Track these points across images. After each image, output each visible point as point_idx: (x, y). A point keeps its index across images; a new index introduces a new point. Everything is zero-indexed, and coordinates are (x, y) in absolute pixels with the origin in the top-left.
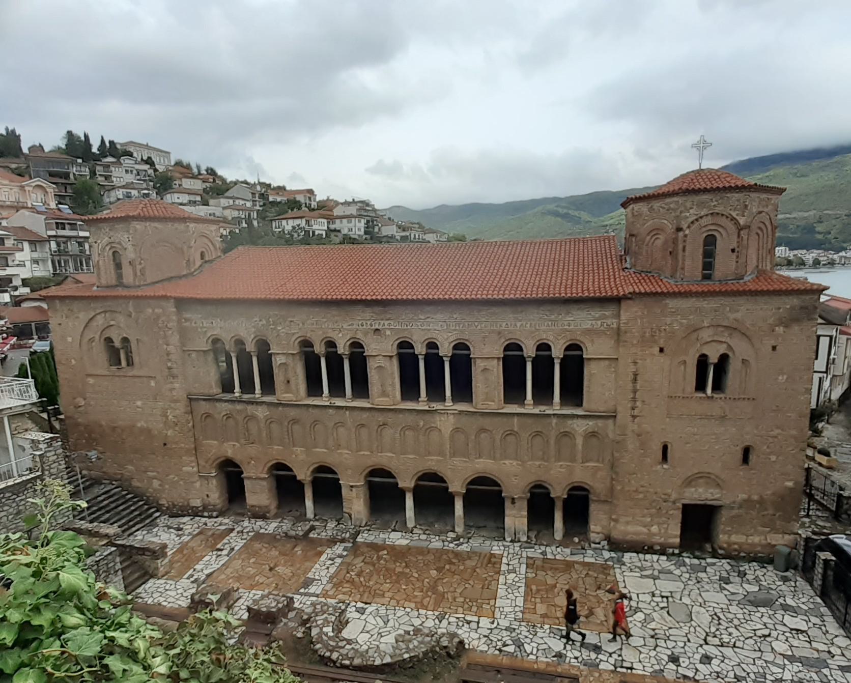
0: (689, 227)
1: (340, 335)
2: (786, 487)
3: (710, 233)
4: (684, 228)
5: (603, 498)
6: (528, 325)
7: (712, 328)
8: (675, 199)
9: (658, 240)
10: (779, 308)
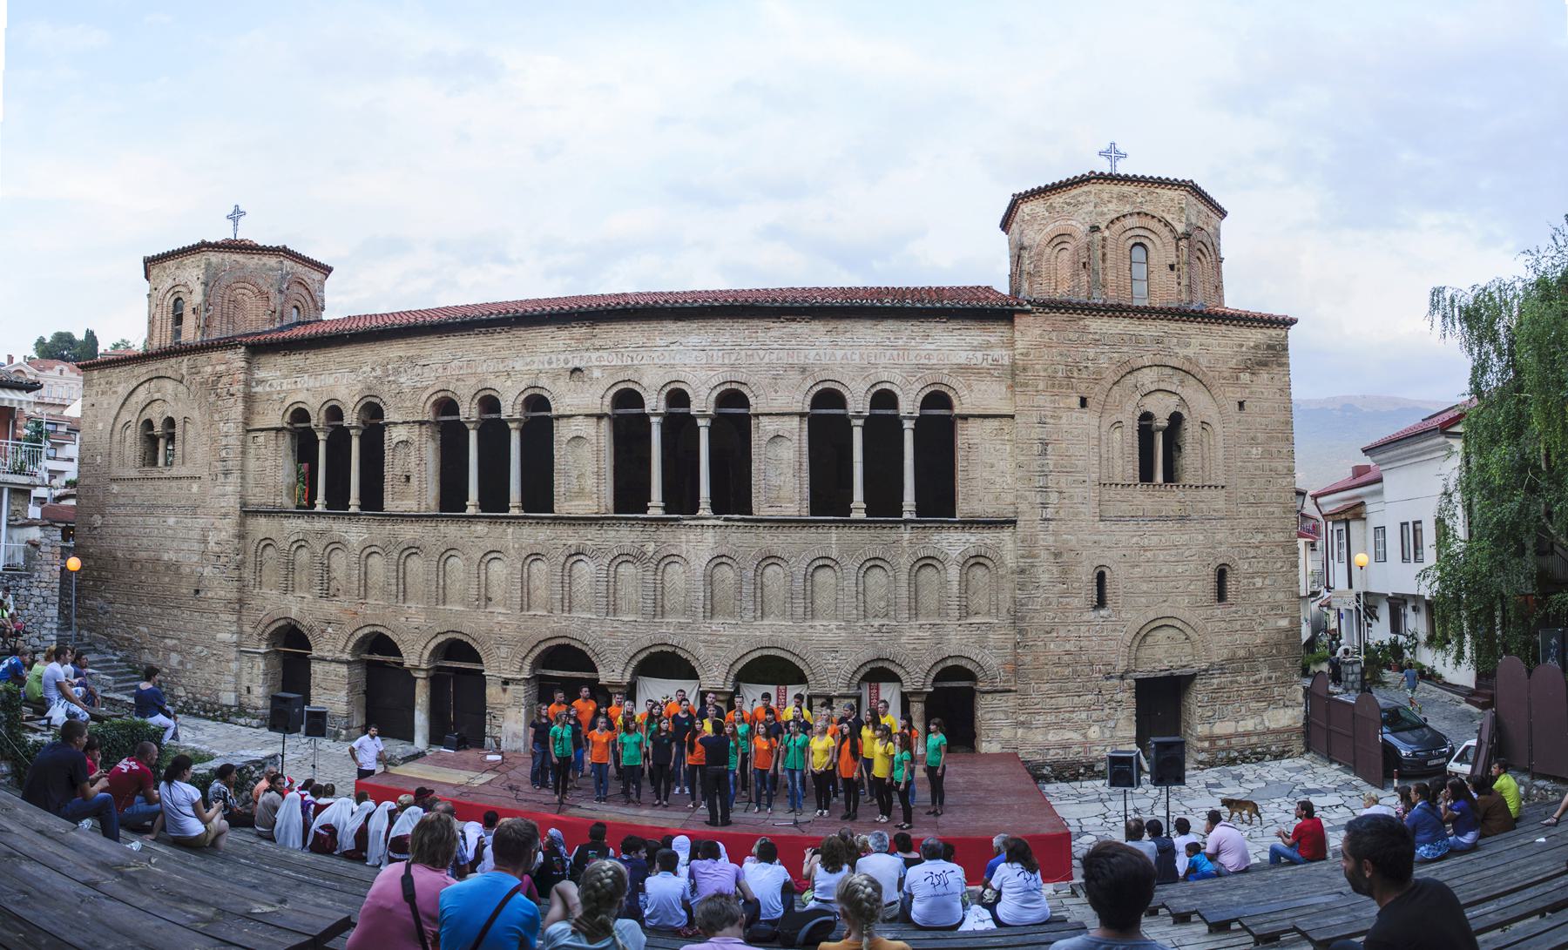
1: (509, 383)
5: (1000, 686)
6: (856, 357)
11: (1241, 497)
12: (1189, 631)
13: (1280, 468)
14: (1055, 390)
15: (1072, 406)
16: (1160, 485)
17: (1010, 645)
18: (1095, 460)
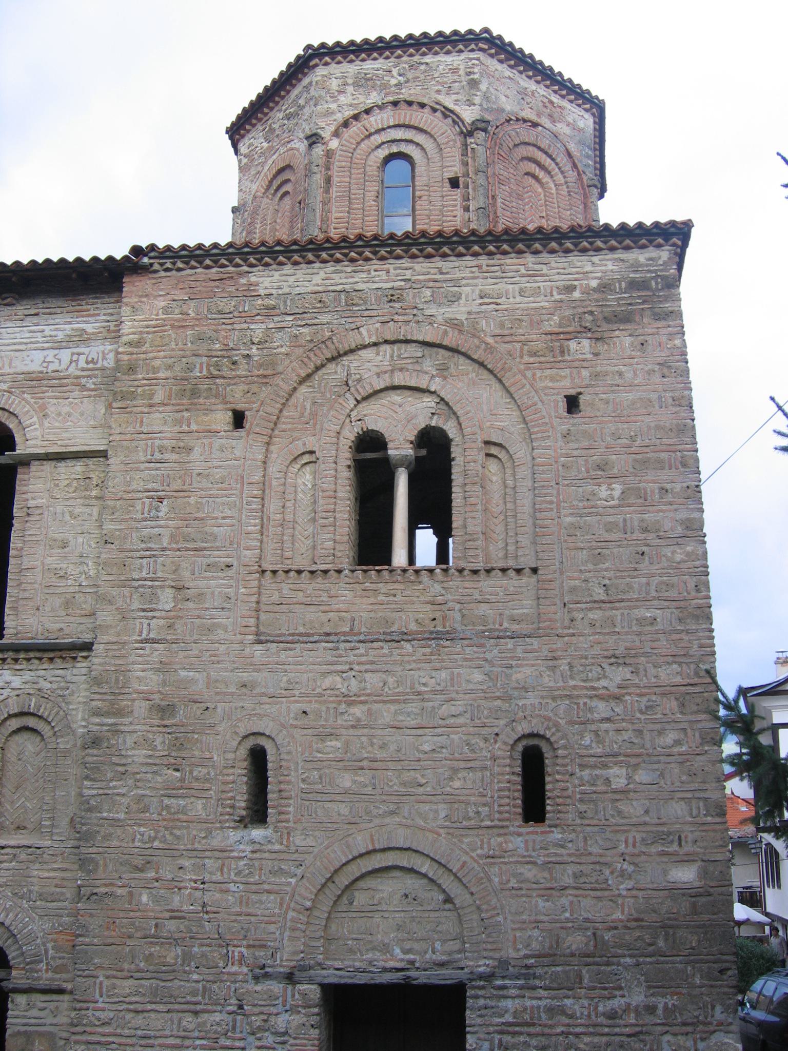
0: (336, 134)
2: (675, 891)
3: (395, 149)
4: (326, 134)
5: (45, 977)
7: (387, 347)
10: (570, 289)
11: (573, 590)
12: (447, 882)
13: (668, 525)
14: (185, 401)
15: (214, 427)
17: (69, 894)
18: (253, 527)
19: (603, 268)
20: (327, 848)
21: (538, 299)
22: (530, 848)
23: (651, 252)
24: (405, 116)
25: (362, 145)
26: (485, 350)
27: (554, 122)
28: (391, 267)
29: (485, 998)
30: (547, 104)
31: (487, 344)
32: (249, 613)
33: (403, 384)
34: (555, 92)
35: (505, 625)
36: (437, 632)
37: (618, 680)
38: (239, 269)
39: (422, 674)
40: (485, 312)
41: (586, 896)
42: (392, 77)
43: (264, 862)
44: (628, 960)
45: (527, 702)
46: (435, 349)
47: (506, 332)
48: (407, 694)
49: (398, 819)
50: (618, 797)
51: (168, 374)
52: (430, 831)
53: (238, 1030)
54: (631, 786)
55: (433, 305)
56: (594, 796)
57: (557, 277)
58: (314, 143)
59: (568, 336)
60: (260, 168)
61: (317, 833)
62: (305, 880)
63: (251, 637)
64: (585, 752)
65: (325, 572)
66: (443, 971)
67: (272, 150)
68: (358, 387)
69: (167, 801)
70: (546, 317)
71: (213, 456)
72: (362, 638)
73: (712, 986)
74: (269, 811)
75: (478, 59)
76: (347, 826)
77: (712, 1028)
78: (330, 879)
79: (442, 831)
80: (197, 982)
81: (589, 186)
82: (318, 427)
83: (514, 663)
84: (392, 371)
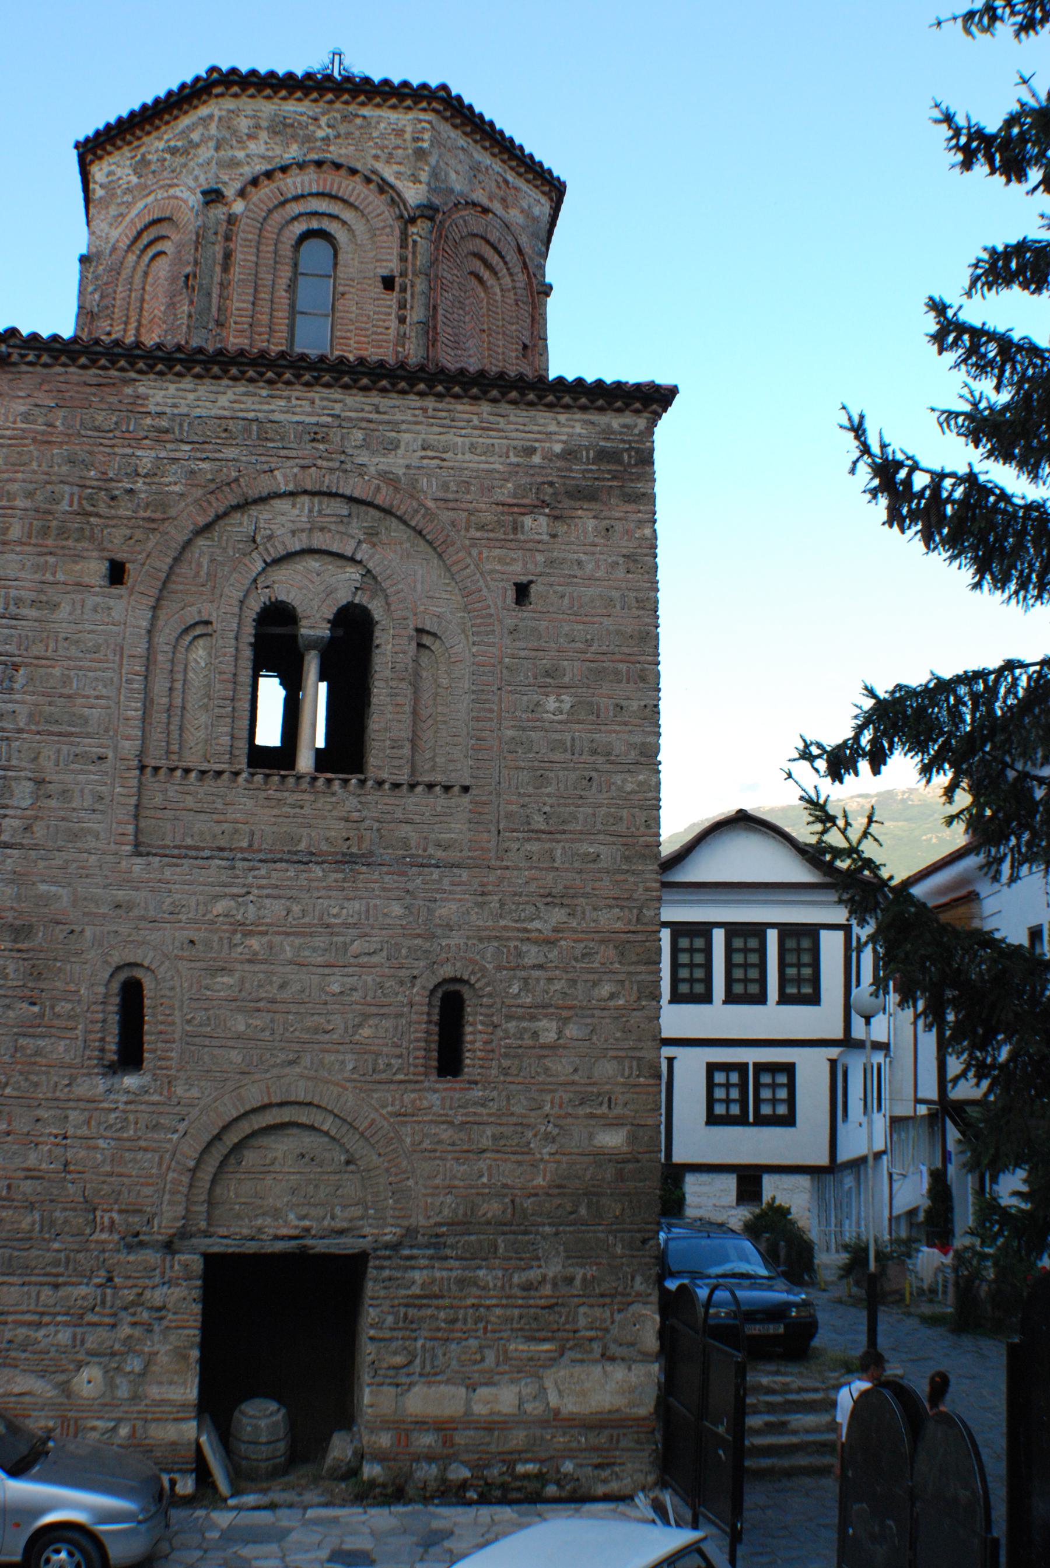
0: (242, 194)
2: (601, 1157)
3: (315, 225)
4: (230, 192)
7: (306, 499)
8: (203, 111)
9: (162, 262)
10: (530, 451)
11: (509, 815)
13: (619, 748)
14: (49, 542)
15: (86, 580)
16: (299, 777)
18: (134, 711)
19: (570, 430)
20: (215, 1100)
21: (492, 459)
22: (447, 1105)
23: (628, 418)
24: (332, 184)
25: (275, 215)
26: (424, 516)
27: (506, 207)
28: (317, 396)
29: (391, 1268)
30: (502, 184)
31: (427, 509)
32: (127, 818)
33: (324, 547)
34: (512, 168)
35: (431, 851)
36: (352, 855)
37: (553, 922)
38: (124, 374)
39: (332, 903)
40: (427, 467)
41: (505, 1161)
42: (320, 127)
43: (139, 1115)
44: (547, 1229)
45: (452, 942)
46: (364, 508)
47: (451, 496)
48: (314, 925)
49: (298, 1070)
50: (545, 1052)
51: (28, 504)
52: (337, 1085)
53: (109, 1304)
54: (561, 1041)
55: (365, 452)
56: (520, 1051)
57: (514, 435)
58: (213, 201)
59: (523, 510)
60: (123, 209)
61: (203, 1083)
62: (188, 1137)
63: (128, 848)
64: (512, 1002)
65: (219, 773)
66: (342, 1240)
67: (144, 190)
68: (268, 545)
69: (22, 1041)
70: (497, 483)
71: (86, 617)
72: (262, 856)
73: (633, 1256)
74: (146, 1055)
75: (429, 122)
76: (238, 1077)
77: (630, 1299)
78: (218, 1137)
79: (348, 1084)
80: (58, 1251)
81: (539, 293)
82: (217, 592)
83: (438, 896)
84: (311, 530)
